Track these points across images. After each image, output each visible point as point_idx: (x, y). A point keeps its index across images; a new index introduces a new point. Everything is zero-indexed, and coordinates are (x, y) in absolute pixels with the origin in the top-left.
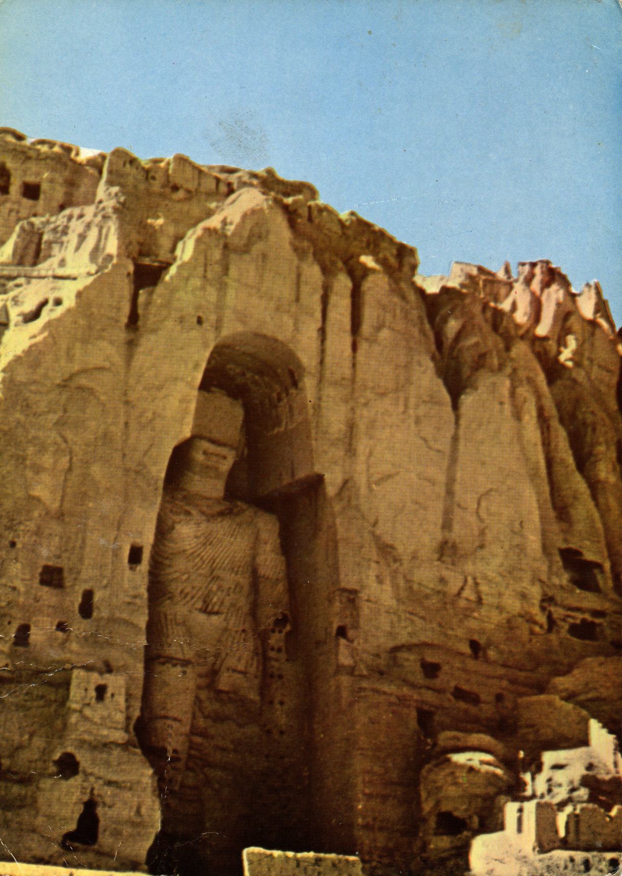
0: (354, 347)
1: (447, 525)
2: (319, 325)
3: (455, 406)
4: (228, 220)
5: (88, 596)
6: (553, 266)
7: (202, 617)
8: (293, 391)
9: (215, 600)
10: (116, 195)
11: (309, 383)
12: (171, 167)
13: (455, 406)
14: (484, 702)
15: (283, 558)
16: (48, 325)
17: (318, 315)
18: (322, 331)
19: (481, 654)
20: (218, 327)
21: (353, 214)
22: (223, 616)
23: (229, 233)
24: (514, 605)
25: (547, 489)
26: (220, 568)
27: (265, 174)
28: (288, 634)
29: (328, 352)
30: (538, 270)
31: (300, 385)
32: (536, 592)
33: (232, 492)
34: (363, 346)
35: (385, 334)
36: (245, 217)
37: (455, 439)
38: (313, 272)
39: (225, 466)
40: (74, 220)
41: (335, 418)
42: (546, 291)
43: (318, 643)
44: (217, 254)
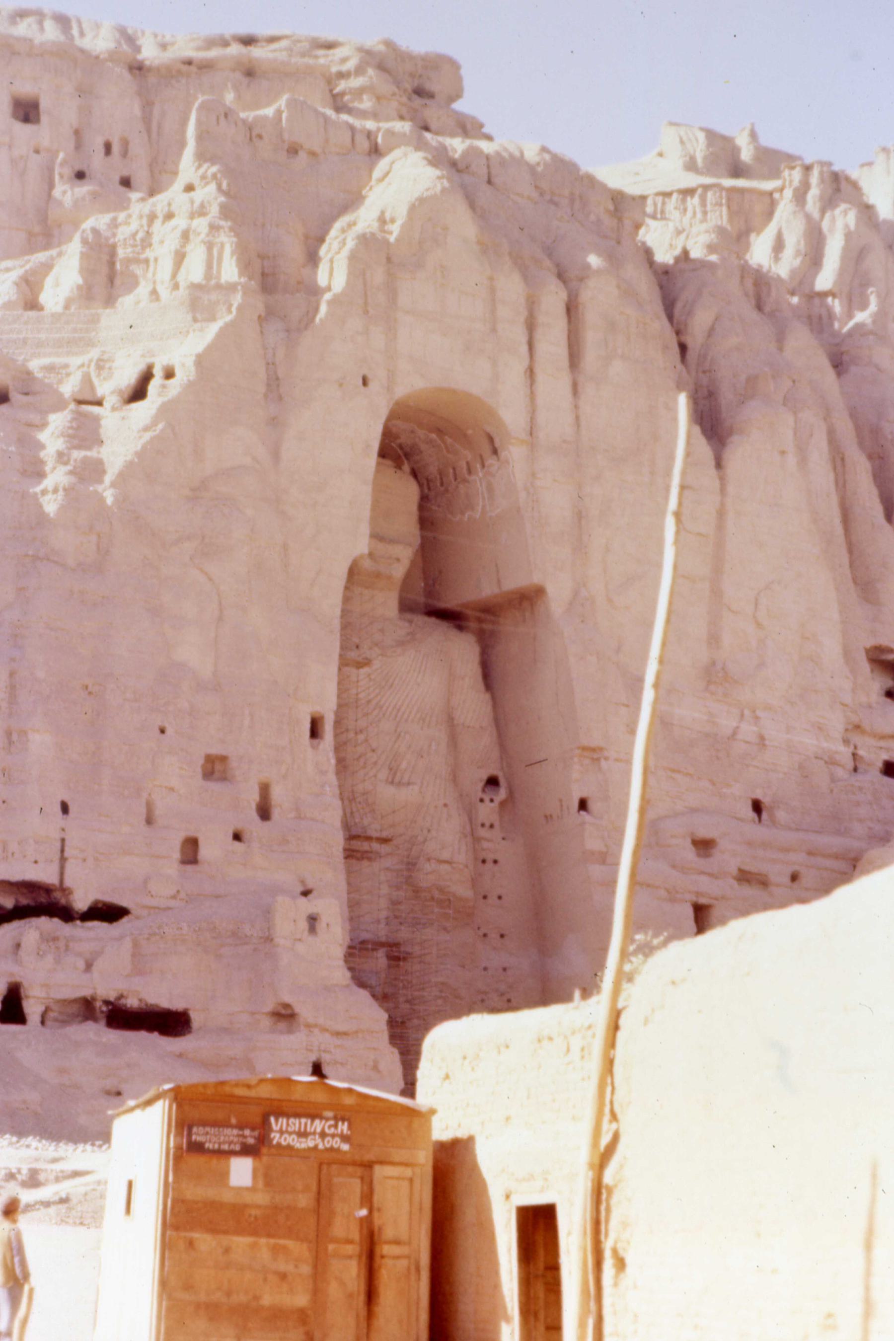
0: (575, 389)
1: (714, 639)
2: (526, 362)
3: (719, 465)
4: (388, 216)
5: (265, 790)
6: (836, 168)
7: (391, 790)
8: (491, 461)
9: (404, 765)
10: (214, 176)
11: (515, 453)
12: (284, 116)
13: (719, 464)
14: (778, 885)
15: (487, 696)
16: (165, 410)
17: (524, 348)
18: (531, 372)
19: (764, 815)
20: (389, 389)
21: (544, 149)
22: (416, 788)
23: (392, 239)
24: (809, 742)
25: (846, 560)
26: (406, 721)
27: (382, 48)
28: (503, 804)
29: (540, 401)
30: (814, 178)
31: (503, 454)
32: (836, 723)
33: (406, 607)
34: (589, 390)
35: (617, 367)
36: (412, 208)
37: (721, 514)
38: (512, 287)
39: (399, 571)
40: (158, 223)
41: (556, 501)
42: (828, 215)
43: (548, 818)
44: (378, 276)
